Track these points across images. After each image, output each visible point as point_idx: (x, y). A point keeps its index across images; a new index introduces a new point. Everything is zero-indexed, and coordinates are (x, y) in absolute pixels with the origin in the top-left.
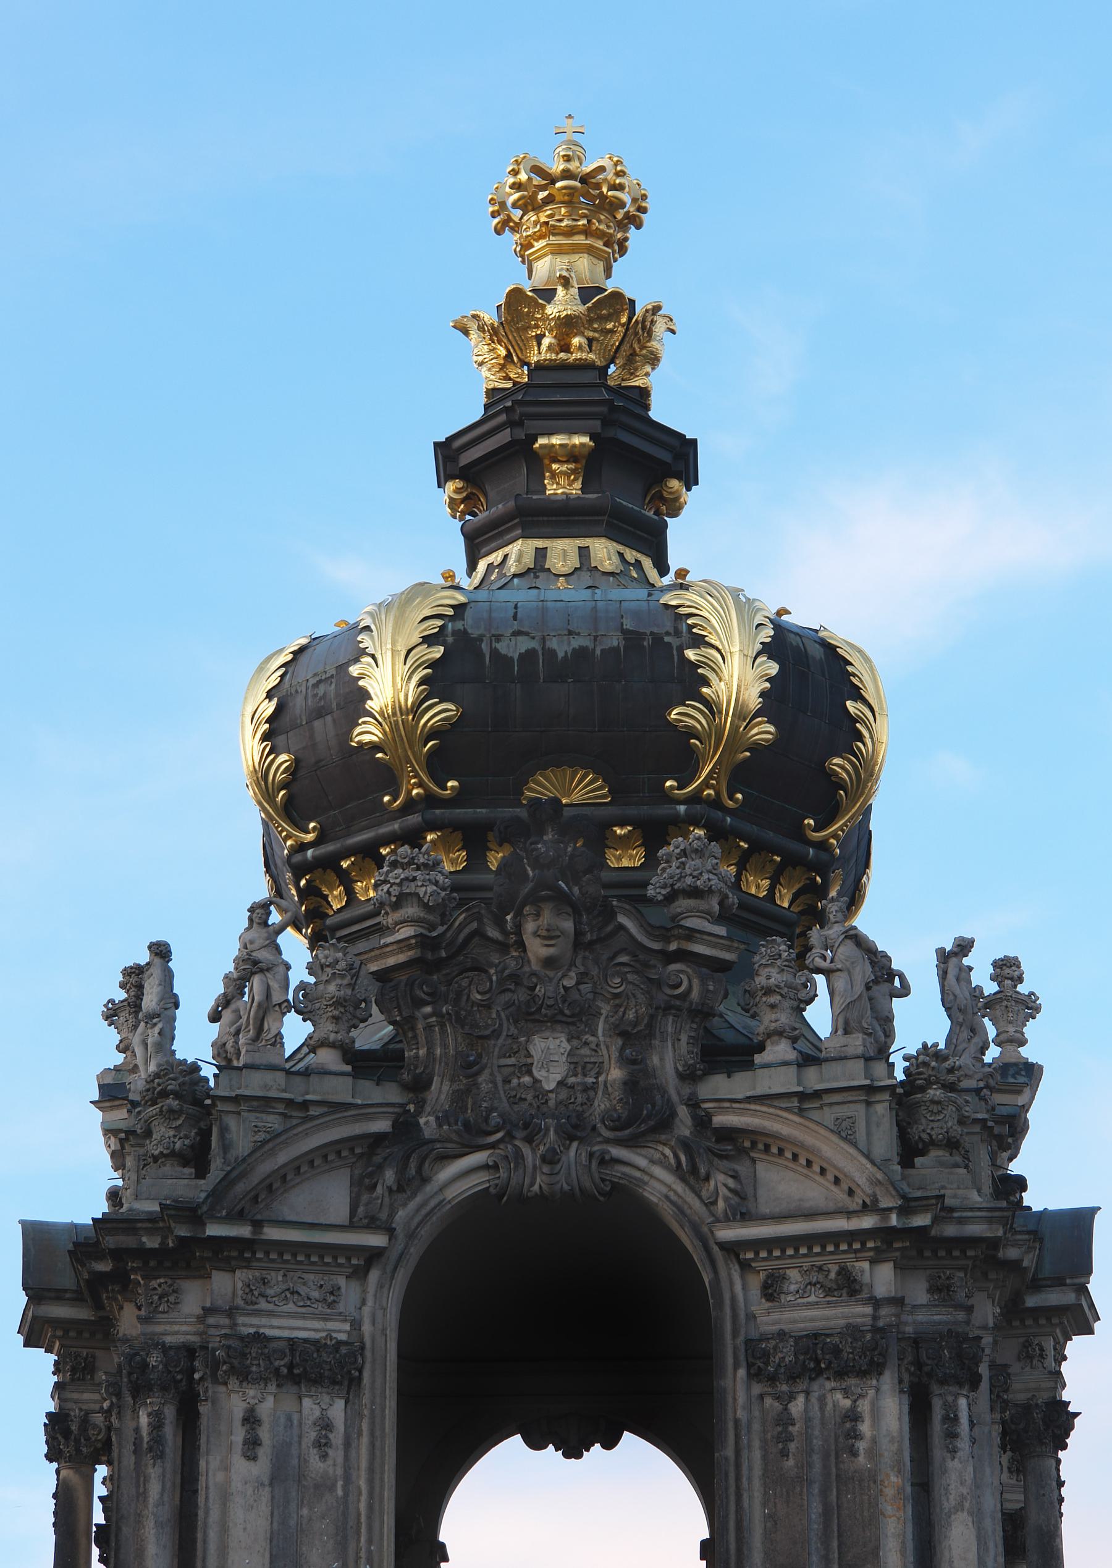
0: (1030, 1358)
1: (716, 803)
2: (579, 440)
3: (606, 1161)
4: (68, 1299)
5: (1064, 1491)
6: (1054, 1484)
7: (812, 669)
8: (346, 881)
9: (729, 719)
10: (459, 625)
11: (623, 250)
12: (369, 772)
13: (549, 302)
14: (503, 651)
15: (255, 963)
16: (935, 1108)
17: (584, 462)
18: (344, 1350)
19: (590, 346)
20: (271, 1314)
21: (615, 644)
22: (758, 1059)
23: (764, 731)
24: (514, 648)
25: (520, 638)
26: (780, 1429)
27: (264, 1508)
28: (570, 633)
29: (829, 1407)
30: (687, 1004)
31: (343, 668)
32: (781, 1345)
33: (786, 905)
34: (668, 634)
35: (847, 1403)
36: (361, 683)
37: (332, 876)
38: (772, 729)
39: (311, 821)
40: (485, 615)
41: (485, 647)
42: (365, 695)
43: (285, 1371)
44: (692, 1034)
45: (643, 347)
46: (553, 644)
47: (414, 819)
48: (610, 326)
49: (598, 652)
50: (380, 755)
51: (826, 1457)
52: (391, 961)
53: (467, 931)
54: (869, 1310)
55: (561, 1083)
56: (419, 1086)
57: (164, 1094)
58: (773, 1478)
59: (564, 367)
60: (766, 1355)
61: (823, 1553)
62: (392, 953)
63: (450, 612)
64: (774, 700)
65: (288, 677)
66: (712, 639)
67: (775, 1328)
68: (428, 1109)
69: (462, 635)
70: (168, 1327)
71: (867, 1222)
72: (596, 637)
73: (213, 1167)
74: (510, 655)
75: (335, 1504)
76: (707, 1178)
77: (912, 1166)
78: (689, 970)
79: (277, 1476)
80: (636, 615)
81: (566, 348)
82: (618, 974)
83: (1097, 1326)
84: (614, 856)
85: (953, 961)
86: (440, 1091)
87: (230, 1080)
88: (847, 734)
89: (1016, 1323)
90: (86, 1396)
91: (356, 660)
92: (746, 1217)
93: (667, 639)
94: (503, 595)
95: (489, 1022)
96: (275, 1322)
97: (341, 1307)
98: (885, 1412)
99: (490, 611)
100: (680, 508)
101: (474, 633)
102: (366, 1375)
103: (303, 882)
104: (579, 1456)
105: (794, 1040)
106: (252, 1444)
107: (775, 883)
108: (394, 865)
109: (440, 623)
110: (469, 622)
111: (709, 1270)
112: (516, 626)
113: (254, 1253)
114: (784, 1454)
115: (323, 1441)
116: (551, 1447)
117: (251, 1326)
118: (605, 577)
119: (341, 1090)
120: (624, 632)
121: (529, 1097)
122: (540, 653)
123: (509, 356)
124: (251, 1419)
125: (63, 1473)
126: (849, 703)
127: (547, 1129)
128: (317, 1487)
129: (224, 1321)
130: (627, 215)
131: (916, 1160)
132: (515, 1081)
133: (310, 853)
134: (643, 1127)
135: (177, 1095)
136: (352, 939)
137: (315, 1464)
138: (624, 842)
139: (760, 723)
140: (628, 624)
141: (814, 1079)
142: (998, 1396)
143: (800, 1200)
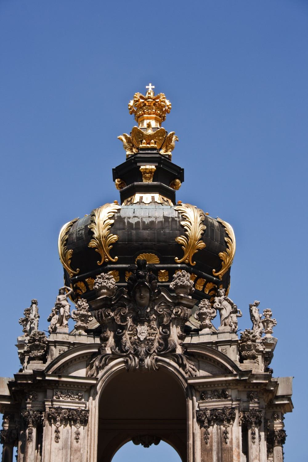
2: (153, 167)
7: (215, 228)
10: (119, 214)
11: (164, 119)
17: (153, 174)
18: (83, 412)
21: (161, 220)
23: (202, 245)
24: (133, 221)
25: (136, 218)
26: (205, 435)
27: (60, 456)
28: (149, 217)
33: (207, 293)
34: (176, 217)
35: (224, 429)
41: (126, 221)
42: (93, 233)
44: (182, 326)
46: (144, 220)
49: (157, 222)
54: (231, 402)
55: (145, 339)
63: (116, 211)
65: (71, 229)
68: (108, 345)
69: (120, 217)
72: (156, 218)
73: (48, 360)
74: (132, 223)
75: (80, 455)
77: (243, 363)
79: (64, 447)
83: (293, 410)
84: (160, 278)
87: (53, 336)
88: (225, 246)
91: (90, 224)
93: (176, 219)
98: (235, 431)
104: (148, 447)
106: (57, 438)
107: (204, 286)
109: (113, 214)
110: (122, 214)
112: (134, 215)
113: (59, 384)
114: (207, 443)
116: (140, 444)
118: (159, 204)
124: (57, 431)
128: (75, 450)
131: (244, 361)
132: (133, 338)
133: (76, 277)
139: (201, 242)
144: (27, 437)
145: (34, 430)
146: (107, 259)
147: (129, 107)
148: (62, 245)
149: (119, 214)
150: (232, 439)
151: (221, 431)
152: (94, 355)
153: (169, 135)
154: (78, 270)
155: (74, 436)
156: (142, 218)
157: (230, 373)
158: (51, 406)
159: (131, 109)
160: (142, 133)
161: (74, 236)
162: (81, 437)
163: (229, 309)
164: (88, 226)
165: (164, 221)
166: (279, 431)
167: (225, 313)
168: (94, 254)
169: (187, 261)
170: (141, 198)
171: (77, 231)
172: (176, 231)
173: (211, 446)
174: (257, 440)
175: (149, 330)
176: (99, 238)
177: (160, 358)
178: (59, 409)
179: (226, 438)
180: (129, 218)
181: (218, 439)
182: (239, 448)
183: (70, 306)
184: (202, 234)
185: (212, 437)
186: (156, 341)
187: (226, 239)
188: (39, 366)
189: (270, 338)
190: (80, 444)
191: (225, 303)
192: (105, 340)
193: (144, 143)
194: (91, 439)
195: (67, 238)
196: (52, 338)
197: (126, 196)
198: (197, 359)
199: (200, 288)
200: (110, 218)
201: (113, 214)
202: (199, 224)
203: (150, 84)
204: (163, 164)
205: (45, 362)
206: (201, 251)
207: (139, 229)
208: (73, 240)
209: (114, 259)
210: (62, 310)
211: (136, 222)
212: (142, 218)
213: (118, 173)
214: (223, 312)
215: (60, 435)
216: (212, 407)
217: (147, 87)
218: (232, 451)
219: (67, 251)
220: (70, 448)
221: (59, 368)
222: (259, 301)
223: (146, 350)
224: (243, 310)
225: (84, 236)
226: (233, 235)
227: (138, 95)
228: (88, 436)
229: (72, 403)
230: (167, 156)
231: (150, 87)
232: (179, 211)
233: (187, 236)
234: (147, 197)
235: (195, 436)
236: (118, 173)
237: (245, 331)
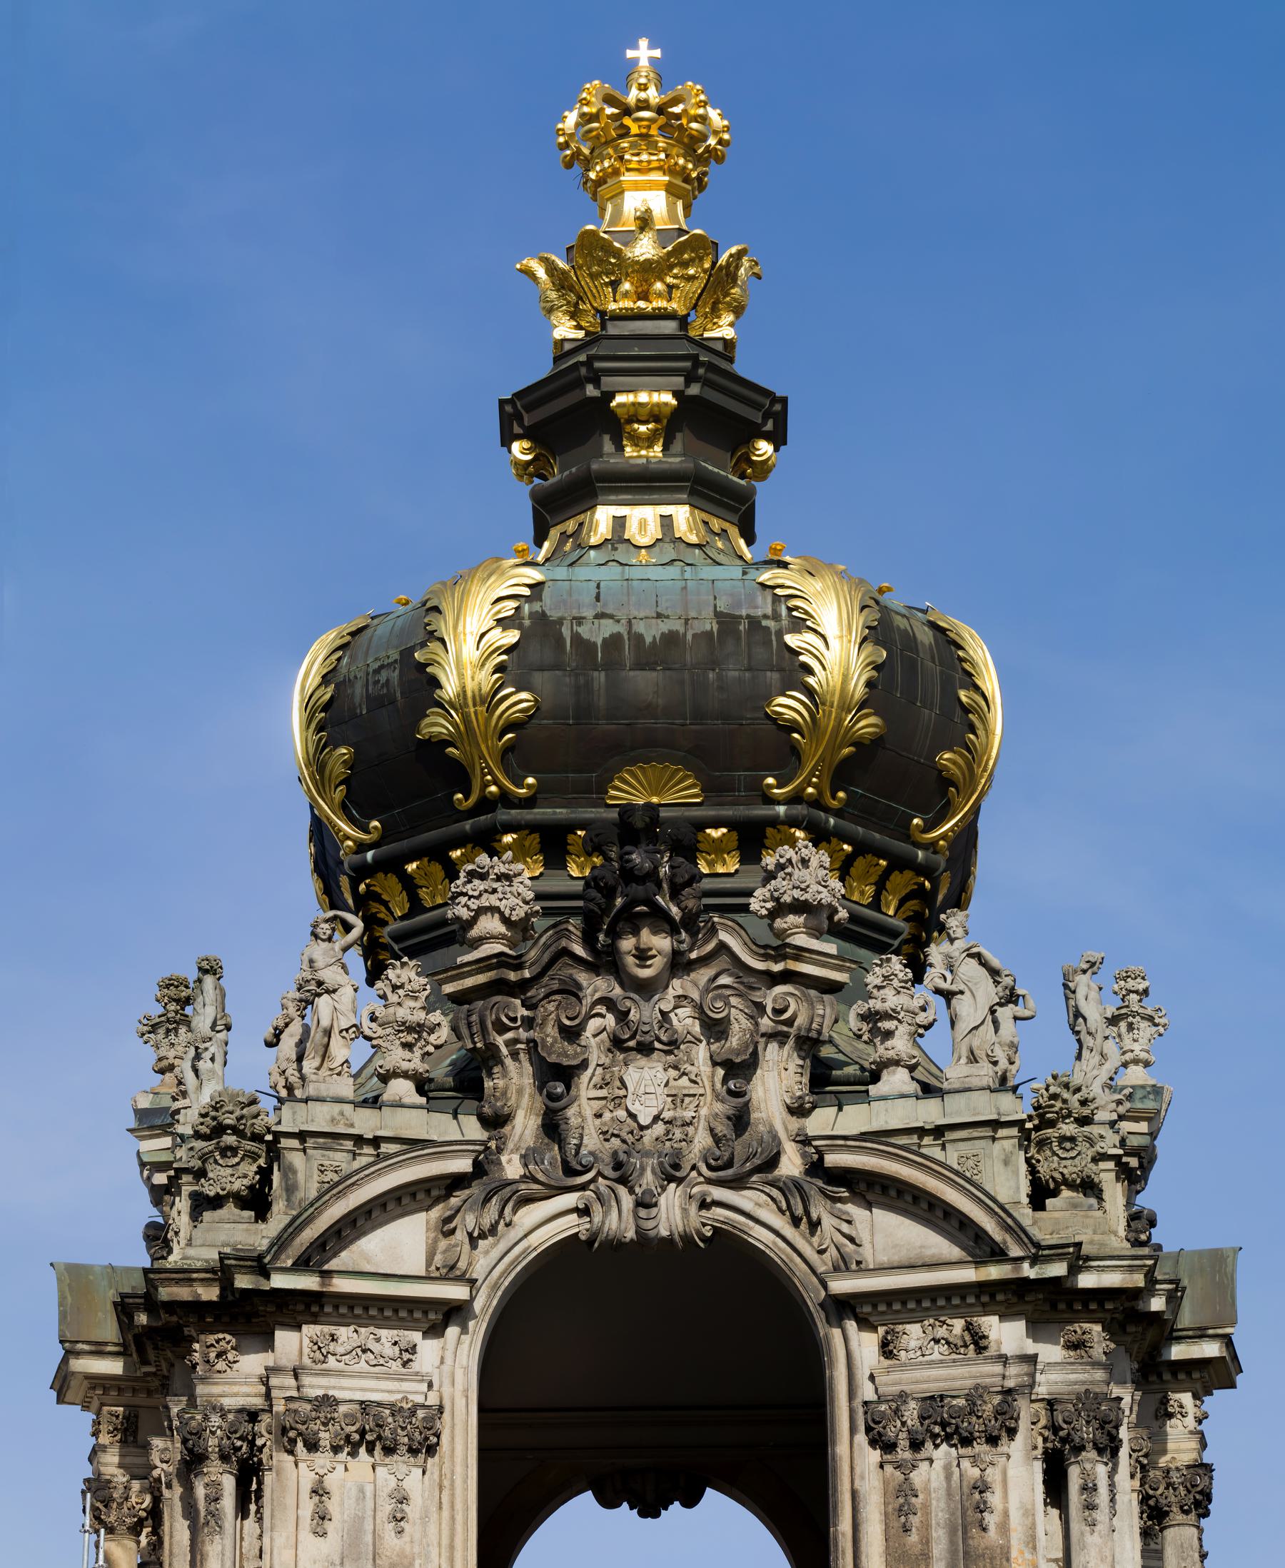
1: (816, 803)
4: (110, 1353)
10: (537, 607)
14: (585, 636)
16: (1068, 1145)
17: (665, 421)
18: (421, 1413)
20: (340, 1374)
21: (708, 627)
23: (868, 725)
25: (603, 621)
26: (901, 1500)
28: (659, 616)
30: (793, 1031)
31: (407, 653)
34: (765, 617)
35: (975, 1472)
36: (429, 670)
37: (393, 880)
39: (372, 818)
41: (566, 632)
42: (435, 683)
43: (356, 1437)
46: (640, 627)
48: (691, 271)
49: (689, 637)
52: (469, 982)
54: (998, 1368)
62: (470, 974)
63: (526, 592)
64: (880, 689)
65: (345, 660)
68: (510, 1145)
72: (687, 620)
73: (275, 1208)
74: (593, 640)
77: (1043, 1208)
84: (706, 860)
87: (294, 1113)
89: (1153, 1378)
91: (423, 645)
93: (764, 623)
97: (415, 1366)
99: (570, 593)
101: (553, 614)
102: (445, 1439)
103: (362, 887)
105: (912, 1069)
107: (880, 886)
108: (472, 875)
110: (548, 604)
113: (322, 1307)
114: (906, 1530)
117: (320, 1387)
118: (690, 550)
120: (718, 614)
122: (626, 637)
124: (319, 1491)
132: (607, 1116)
137: (391, 1542)
138: (718, 848)
139: (866, 716)
140: (722, 607)
143: (921, 1247)
144: (203, 1513)
145: (229, 1483)
146: (493, 789)
147: (561, 139)
148: (308, 727)
149: (539, 604)
150: (1006, 1514)
151: (965, 1484)
152: (456, 1182)
153: (723, 259)
154: (375, 828)
155: (387, 1507)
156: (630, 622)
157: (997, 1254)
158: (295, 1394)
159: (566, 145)
160: (618, 254)
161: (359, 690)
162: (412, 1510)
163: (987, 992)
166: (1188, 1467)
167: (970, 1010)
168: (441, 768)
169: (810, 790)
170: (620, 522)
171: (371, 670)
172: (769, 674)
173: (926, 1541)
174: (1102, 1515)
175: (672, 1083)
176: (460, 703)
177: (718, 1193)
178: (326, 1402)
179: (982, 1508)
180: (579, 620)
181: (953, 1514)
182: (1034, 1548)
184: (870, 684)
185: (926, 1506)
186: (702, 1125)
187: (963, 695)
188: (235, 1231)
189: (1143, 1087)
191: (970, 969)
192: (495, 1122)
193: (626, 295)
194: (453, 1519)
195: (328, 696)
196: (292, 1118)
197: (556, 506)
198: (864, 1197)
199: (862, 893)
200: (502, 623)
202: (859, 640)
203: (643, 43)
204: (707, 383)
206: (867, 749)
207: (621, 666)
209: (520, 786)
210: (323, 1003)
212: (630, 622)
213: (516, 416)
214: (963, 1005)
215: (333, 1506)
216: (925, 1386)
217: (630, 54)
218: (1008, 1560)
220: (371, 1557)
223: (661, 1164)
224: (1042, 997)
225: (398, 694)
226: (990, 682)
227: (593, 90)
228: (441, 1508)
229: (377, 1377)
230: (719, 347)
231: (643, 53)
232: (779, 592)
233: (810, 692)
234: (643, 520)
235: (861, 1505)
236: (516, 416)
237: (1050, 1080)
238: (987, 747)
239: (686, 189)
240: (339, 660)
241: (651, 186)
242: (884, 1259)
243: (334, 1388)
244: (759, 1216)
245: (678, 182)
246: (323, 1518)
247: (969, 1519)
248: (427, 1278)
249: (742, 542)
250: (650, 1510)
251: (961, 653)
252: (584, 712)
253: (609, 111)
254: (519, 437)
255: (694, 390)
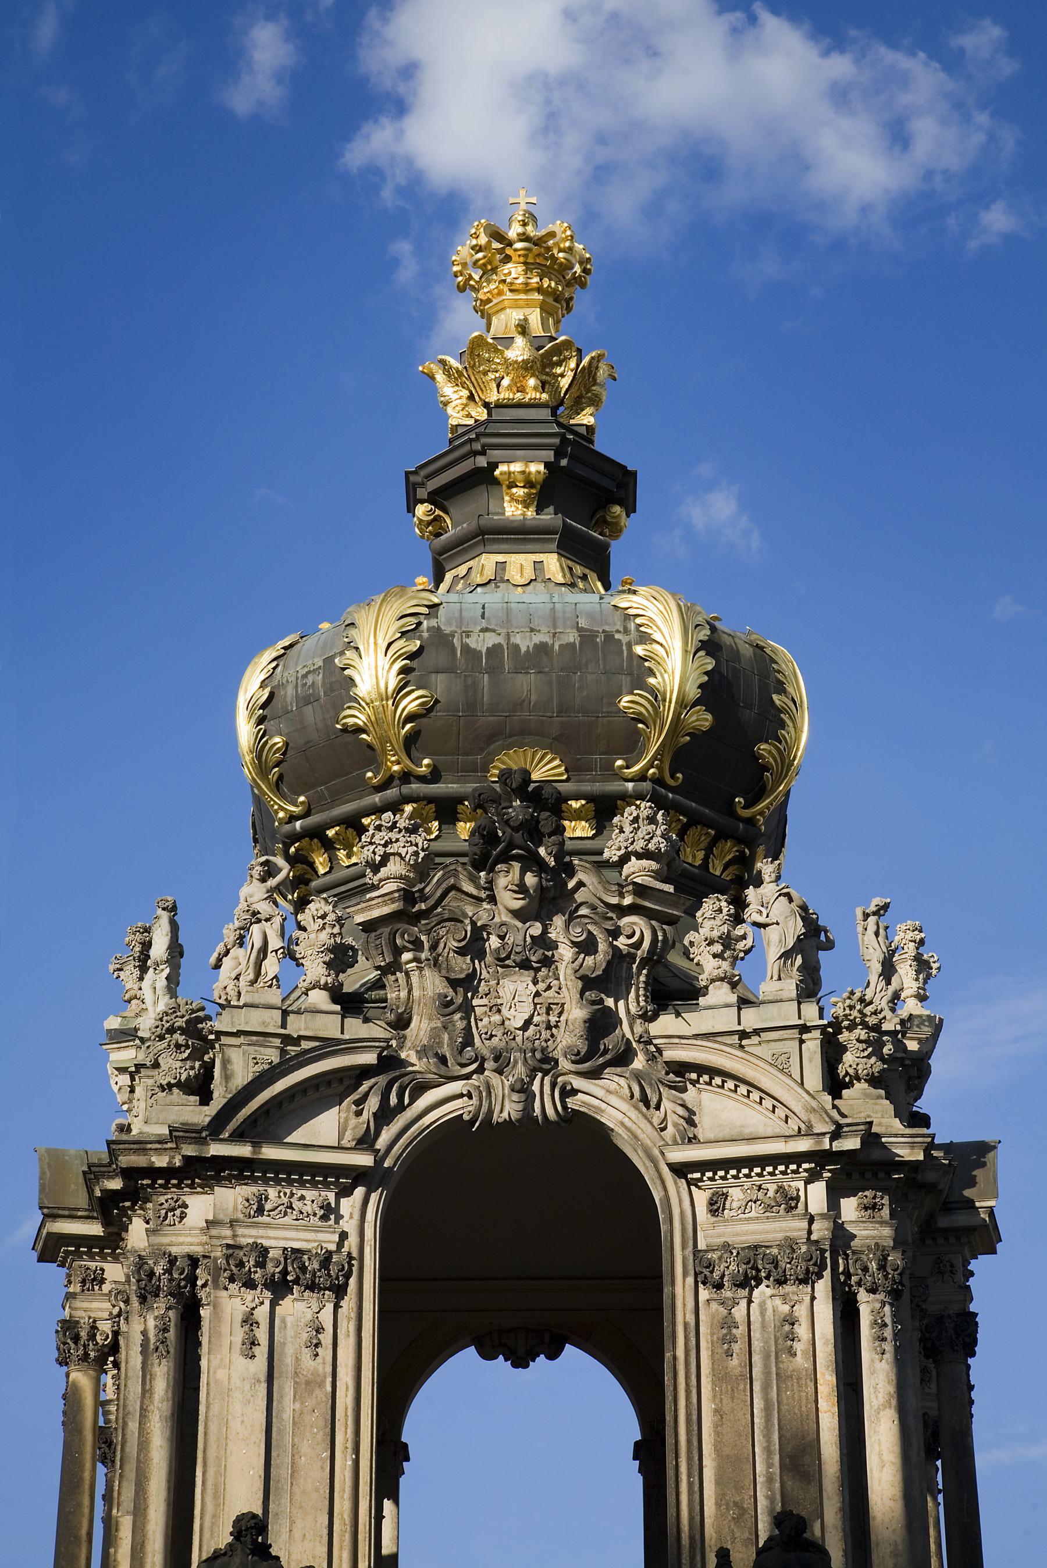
0: (941, 1273)
1: (658, 781)
3: (568, 1092)
4: (80, 1217)
5: (974, 1395)
6: (965, 1387)
8: (328, 846)
9: (673, 705)
10: (433, 623)
12: (352, 750)
13: (507, 349)
14: (473, 646)
15: (255, 913)
19: (543, 388)
20: (267, 1226)
21: (572, 640)
22: (702, 1001)
24: (481, 643)
25: (487, 634)
26: (725, 1331)
28: (532, 630)
29: (769, 1312)
31: (329, 661)
32: (725, 1256)
33: (718, 873)
38: (709, 717)
39: (299, 795)
40: (457, 614)
41: (456, 642)
45: (588, 391)
46: (517, 639)
47: (392, 793)
49: (556, 647)
50: (364, 736)
51: (766, 1357)
52: (376, 913)
53: (444, 886)
56: (402, 1023)
57: (171, 1031)
58: (721, 1377)
59: (520, 405)
60: (710, 1265)
61: (765, 1445)
63: (425, 610)
65: (279, 668)
66: (657, 636)
67: (720, 1241)
68: (408, 1044)
70: (174, 1239)
71: (803, 1145)
73: (215, 1095)
74: (478, 649)
75: (324, 1399)
76: (658, 1107)
77: (840, 1097)
78: (641, 922)
80: (590, 616)
81: (522, 390)
82: (579, 924)
83: (999, 1246)
85: (872, 919)
86: (420, 1028)
87: (232, 1017)
88: (773, 722)
89: (929, 1242)
90: (95, 1305)
92: (693, 1140)
93: (617, 636)
94: (471, 598)
95: (464, 967)
96: (272, 1233)
100: (621, 531)
101: (447, 630)
103: (292, 849)
104: (526, 1366)
105: (734, 985)
107: (709, 851)
108: (378, 828)
111: (660, 1188)
115: (315, 1341)
117: (250, 1236)
118: (558, 588)
119: (329, 1026)
120: (580, 630)
121: (499, 1034)
122: (505, 647)
123: (471, 397)
124: (249, 1321)
125: (73, 1375)
126: (775, 697)
127: (516, 1062)
128: (308, 1383)
129: (228, 1232)
130: (574, 277)
131: (844, 1091)
133: (298, 824)
134: (601, 1060)
135: (183, 1031)
136: (342, 897)
138: (577, 816)
140: (583, 623)
141: (751, 1019)
142: (918, 1306)
143: (742, 1126)
147: (455, 269)
152: (364, 1072)
153: (585, 361)
158: (230, 1242)
161: (290, 691)
164: (336, 661)
165: (581, 643)
170: (501, 566)
171: (300, 675)
181: (766, 1342)
183: (284, 920)
189: (920, 1016)
190: (324, 1363)
195: (267, 695)
199: (694, 857)
201: (413, 620)
202: (693, 651)
205: (206, 1098)
208: (287, 706)
211: (490, 645)
212: (508, 634)
219: (266, 742)
221: (253, 1120)
222: (888, 900)
229: (297, 1229)
230: (583, 431)
234: (519, 564)
238: (798, 739)
239: (556, 305)
240: (274, 668)
241: (528, 304)
242: (711, 1136)
243: (262, 1237)
244: (609, 1100)
245: (550, 300)
246: (253, 1343)
247: (780, 1347)
248: (340, 1148)
249: (599, 584)
250: (521, 1361)
251: (775, 666)
252: (472, 706)
253: (496, 245)
254: (422, 502)
255: (564, 462)
